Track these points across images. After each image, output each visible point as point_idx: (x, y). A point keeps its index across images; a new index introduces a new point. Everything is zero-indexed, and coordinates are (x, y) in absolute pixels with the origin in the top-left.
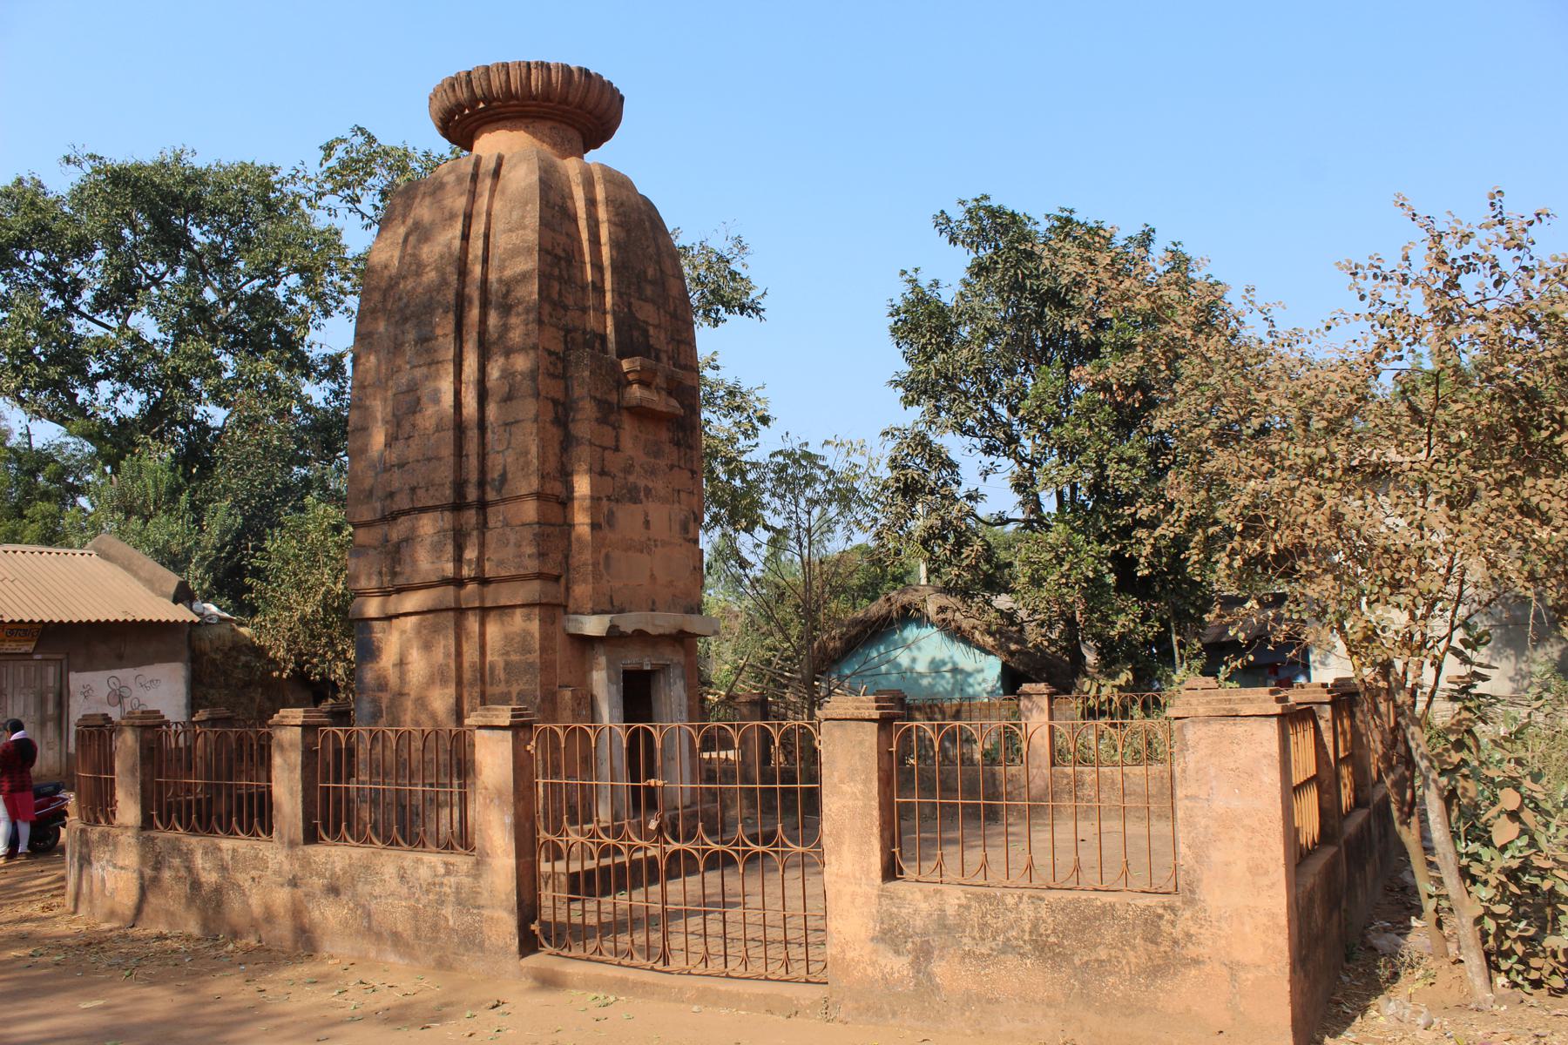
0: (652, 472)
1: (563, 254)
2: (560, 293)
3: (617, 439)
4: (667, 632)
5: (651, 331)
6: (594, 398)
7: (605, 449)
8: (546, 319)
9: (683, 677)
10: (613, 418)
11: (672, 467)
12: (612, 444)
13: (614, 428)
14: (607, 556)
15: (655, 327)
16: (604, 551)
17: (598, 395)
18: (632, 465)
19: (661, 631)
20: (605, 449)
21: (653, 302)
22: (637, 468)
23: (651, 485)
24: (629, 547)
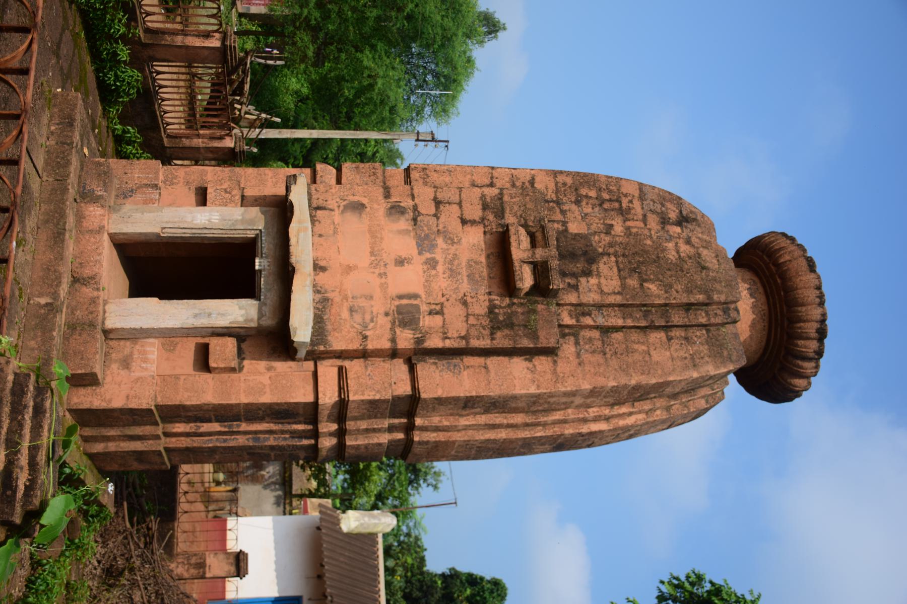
0: (453, 273)
1: (624, 205)
2: (587, 196)
3: (473, 222)
4: (292, 249)
5: (593, 281)
6: (501, 194)
7: (460, 204)
8: (560, 179)
9: (246, 321)
10: (491, 217)
11: (465, 303)
12: (468, 217)
13: (483, 219)
14: (363, 206)
15: (599, 285)
16: (365, 201)
17: (506, 198)
18: (453, 243)
19: (293, 241)
20: (460, 204)
21: (623, 286)
22: (453, 249)
23: (440, 268)
24: (374, 235)
